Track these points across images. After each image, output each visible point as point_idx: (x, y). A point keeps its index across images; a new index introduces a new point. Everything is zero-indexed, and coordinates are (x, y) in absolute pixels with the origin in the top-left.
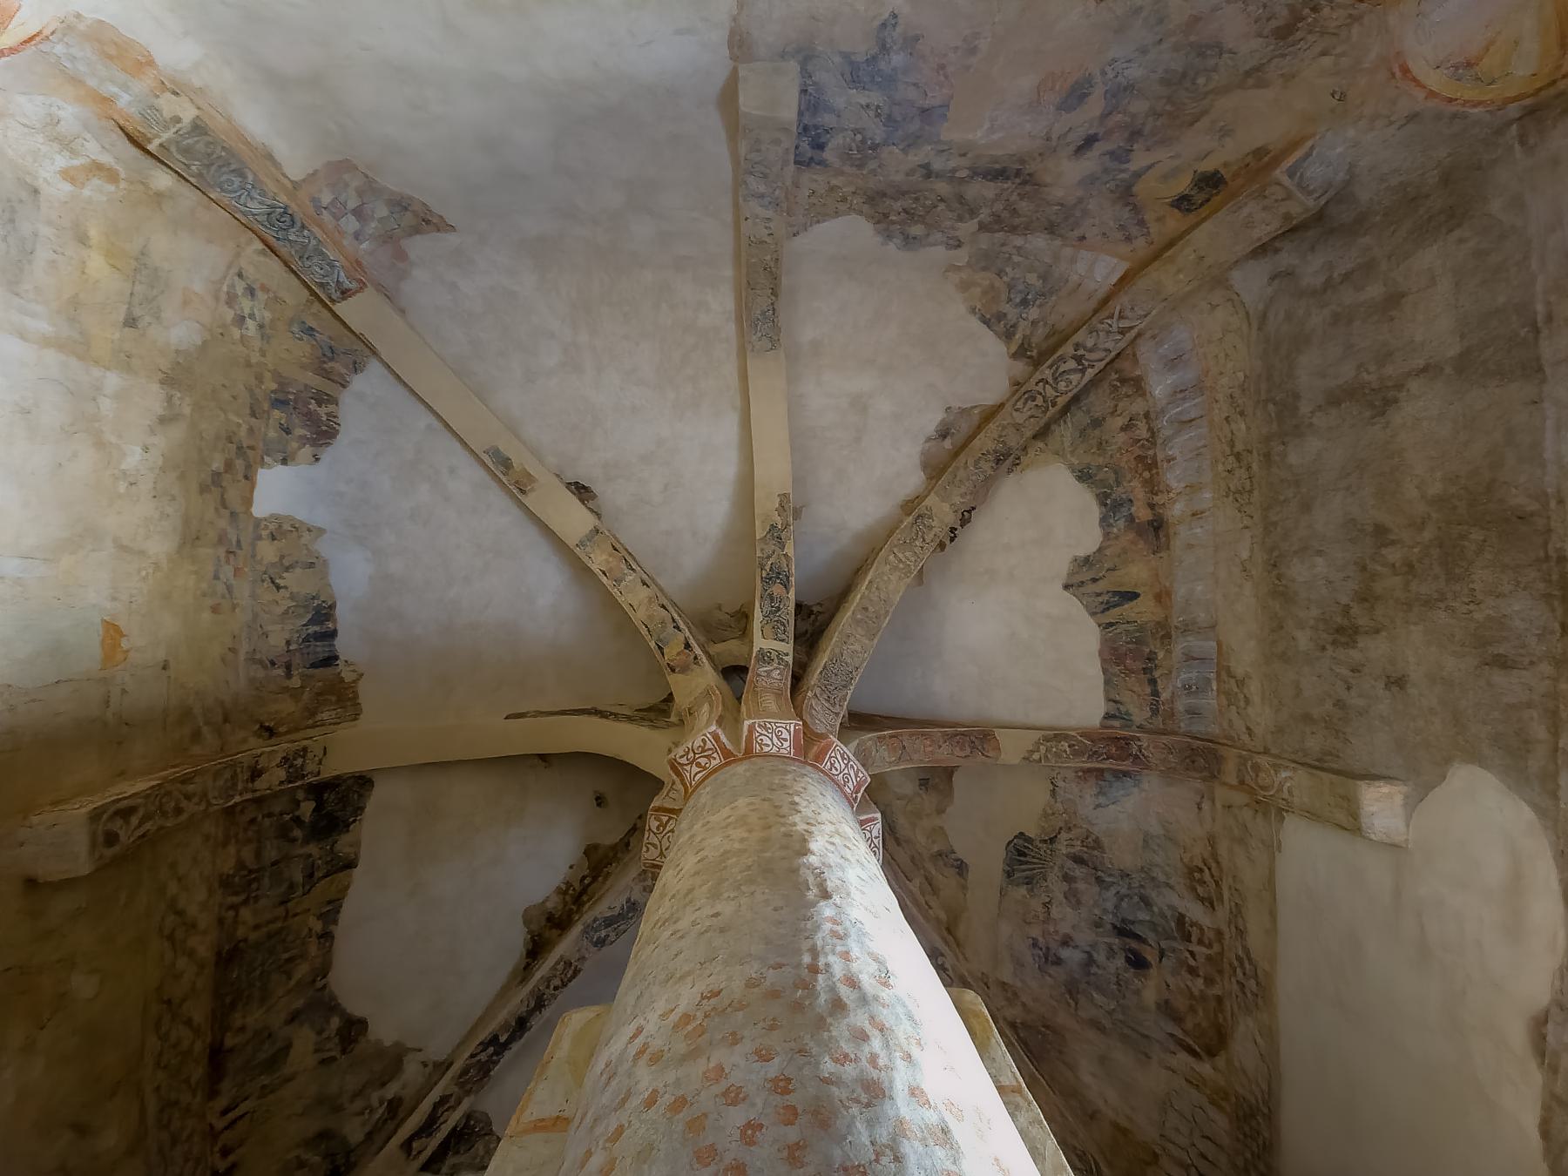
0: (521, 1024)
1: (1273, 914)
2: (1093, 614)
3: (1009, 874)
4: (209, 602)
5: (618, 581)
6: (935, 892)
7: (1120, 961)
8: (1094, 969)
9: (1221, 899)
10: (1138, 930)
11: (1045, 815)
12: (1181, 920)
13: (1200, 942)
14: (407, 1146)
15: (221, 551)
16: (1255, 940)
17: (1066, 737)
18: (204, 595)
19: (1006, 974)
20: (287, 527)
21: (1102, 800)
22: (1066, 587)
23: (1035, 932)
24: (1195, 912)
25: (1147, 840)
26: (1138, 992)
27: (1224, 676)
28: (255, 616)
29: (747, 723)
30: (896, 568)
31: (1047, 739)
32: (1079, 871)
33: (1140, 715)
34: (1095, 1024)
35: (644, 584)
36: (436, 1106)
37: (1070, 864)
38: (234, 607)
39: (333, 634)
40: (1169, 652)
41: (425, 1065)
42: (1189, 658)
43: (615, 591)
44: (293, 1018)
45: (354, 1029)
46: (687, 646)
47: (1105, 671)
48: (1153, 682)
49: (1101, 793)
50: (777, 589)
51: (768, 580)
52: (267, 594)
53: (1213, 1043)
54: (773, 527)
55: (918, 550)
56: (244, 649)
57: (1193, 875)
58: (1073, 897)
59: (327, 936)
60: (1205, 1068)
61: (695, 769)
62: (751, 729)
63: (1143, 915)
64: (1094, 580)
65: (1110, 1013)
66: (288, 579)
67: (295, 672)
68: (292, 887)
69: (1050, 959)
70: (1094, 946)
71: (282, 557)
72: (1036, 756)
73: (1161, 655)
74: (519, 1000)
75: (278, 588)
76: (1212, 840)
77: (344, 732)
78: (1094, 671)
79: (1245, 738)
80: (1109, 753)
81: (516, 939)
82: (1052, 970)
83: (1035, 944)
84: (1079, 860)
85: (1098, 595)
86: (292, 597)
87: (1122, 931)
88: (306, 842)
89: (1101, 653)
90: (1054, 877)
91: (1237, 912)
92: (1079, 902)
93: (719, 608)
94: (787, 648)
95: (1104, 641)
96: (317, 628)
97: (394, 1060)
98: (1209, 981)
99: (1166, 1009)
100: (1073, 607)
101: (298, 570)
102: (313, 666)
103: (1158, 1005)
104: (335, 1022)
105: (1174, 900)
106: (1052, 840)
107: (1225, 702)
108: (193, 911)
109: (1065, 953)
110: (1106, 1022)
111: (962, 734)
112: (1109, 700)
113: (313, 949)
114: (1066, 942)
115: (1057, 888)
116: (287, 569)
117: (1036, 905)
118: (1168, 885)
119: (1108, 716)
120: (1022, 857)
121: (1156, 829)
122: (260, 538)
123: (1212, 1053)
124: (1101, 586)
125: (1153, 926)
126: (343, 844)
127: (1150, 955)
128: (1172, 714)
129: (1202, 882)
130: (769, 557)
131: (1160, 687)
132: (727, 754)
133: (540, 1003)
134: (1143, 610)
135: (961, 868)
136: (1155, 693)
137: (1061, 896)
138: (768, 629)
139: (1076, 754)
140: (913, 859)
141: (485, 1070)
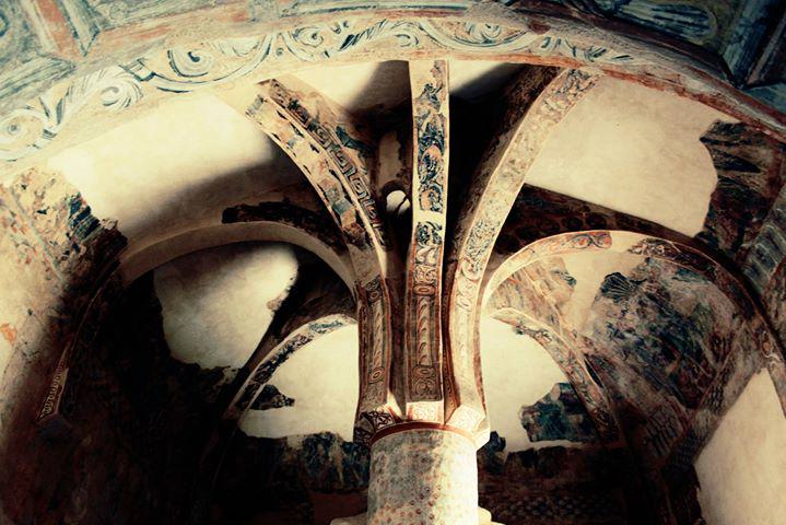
0: (282, 358)
1: (741, 390)
2: (717, 167)
3: (604, 291)
4: (23, 261)
5: (291, 145)
7: (658, 350)
8: (642, 347)
9: (723, 361)
10: (675, 342)
11: (638, 268)
12: (700, 351)
13: (705, 367)
15: (9, 229)
16: (728, 390)
17: (664, 243)
18: (19, 261)
19: (589, 334)
21: (678, 276)
22: (703, 140)
23: (613, 321)
24: (709, 355)
25: (698, 307)
26: (663, 366)
27: (782, 271)
28: (45, 240)
29: (408, 405)
30: (547, 116)
31: (650, 241)
33: (723, 244)
35: (314, 149)
38: (34, 249)
39: (88, 210)
40: (760, 223)
41: (234, 370)
42: (770, 237)
43: (289, 153)
46: (359, 220)
47: (711, 207)
48: (741, 233)
50: (433, 151)
51: (425, 142)
52: (42, 221)
53: (693, 404)
54: (428, 87)
55: (570, 98)
56: (51, 260)
57: (714, 340)
58: (642, 313)
60: (683, 409)
61: (379, 421)
62: (411, 408)
64: (728, 144)
65: (644, 367)
66: (48, 202)
67: (80, 246)
69: (617, 334)
70: (647, 338)
71: (36, 193)
72: (638, 250)
73: (755, 220)
74: (278, 349)
75: (44, 212)
76: (732, 335)
77: (125, 257)
79: (773, 316)
80: (694, 254)
81: (267, 318)
82: (618, 340)
83: (610, 326)
84: (651, 297)
85: (726, 155)
86: (55, 209)
89: (712, 195)
91: (727, 373)
92: (645, 317)
93: (381, 106)
94: (440, 219)
95: (718, 189)
96: (77, 213)
97: (219, 371)
98: (700, 383)
99: (674, 377)
100: (704, 156)
101: (48, 191)
102: (87, 234)
103: (671, 375)
105: (701, 342)
106: (639, 283)
107: (774, 284)
108: (105, 382)
109: (627, 335)
110: (641, 370)
111: (585, 235)
112: (706, 225)
114: (630, 331)
115: (633, 304)
116: (42, 197)
117: (617, 309)
118: (700, 333)
119: (701, 234)
121: (705, 304)
122: (19, 196)
123: (688, 407)
124: (733, 150)
125: (684, 344)
128: (744, 259)
129: (718, 345)
130: (424, 117)
132: (397, 420)
133: (291, 350)
134: (758, 182)
135: (572, 281)
136: (740, 240)
137: (635, 311)
138: (425, 198)
139: (668, 255)
140: (538, 271)
141: (268, 374)
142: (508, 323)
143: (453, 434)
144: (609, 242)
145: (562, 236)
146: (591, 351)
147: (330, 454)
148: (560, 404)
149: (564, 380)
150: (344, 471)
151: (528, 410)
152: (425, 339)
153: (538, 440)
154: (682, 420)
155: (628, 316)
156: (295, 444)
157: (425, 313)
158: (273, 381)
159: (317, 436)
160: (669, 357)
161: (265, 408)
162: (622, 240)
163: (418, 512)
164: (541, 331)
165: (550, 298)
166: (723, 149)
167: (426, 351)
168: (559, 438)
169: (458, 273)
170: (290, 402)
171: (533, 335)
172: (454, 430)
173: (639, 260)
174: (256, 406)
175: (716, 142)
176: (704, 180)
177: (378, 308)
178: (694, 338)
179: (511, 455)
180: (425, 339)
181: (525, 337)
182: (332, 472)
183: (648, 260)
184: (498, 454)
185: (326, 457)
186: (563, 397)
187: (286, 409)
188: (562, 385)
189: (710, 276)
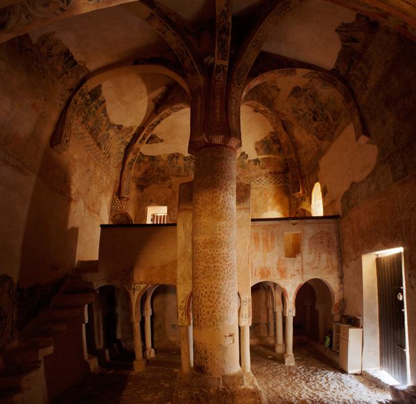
0: (158, 122)
2: (342, 41)
3: (292, 94)
6: (270, 93)
7: (311, 118)
11: (306, 85)
14: (140, 142)
19: (284, 112)
20: (44, 38)
22: (336, 30)
31: (311, 72)
32: (310, 98)
34: (301, 126)
36: (144, 136)
37: (308, 96)
44: (107, 130)
45: (120, 127)
49: (323, 85)
59: (106, 115)
60: (318, 141)
63: (321, 112)
64: (347, 32)
68: (94, 112)
78: (335, 57)
84: (311, 96)
85: (346, 36)
87: (314, 112)
88: (92, 103)
89: (339, 53)
90: (303, 99)
97: (131, 129)
100: (337, 38)
104: (115, 127)
112: (336, 65)
113: (104, 118)
114: (301, 110)
119: (333, 69)
120: (296, 91)
126: (100, 99)
127: (318, 120)
131: (351, 69)
132: (206, 143)
133: (162, 119)
141: (152, 129)
142: (252, 107)
143: (228, 149)
144: (295, 74)
145: (276, 71)
146: (284, 119)
147: (179, 162)
148: (270, 140)
149: (273, 130)
150: (184, 169)
151: (257, 143)
152: (218, 111)
153: (261, 155)
154: (317, 146)
155: (301, 104)
156: (165, 158)
157: (218, 101)
158: (154, 132)
159: (173, 154)
160: (315, 119)
161: (151, 143)
162: (301, 72)
163: (213, 178)
164: (265, 110)
165: (270, 97)
166: (344, 33)
167: (218, 116)
168: (269, 154)
169: (232, 85)
170: (162, 141)
171: (261, 112)
172: (229, 147)
173: (307, 80)
174: (147, 143)
175: (342, 31)
176: (336, 47)
177: (199, 99)
178: (326, 112)
179: (249, 161)
180: (218, 111)
181: (258, 114)
182: (179, 170)
183: (311, 81)
184: (245, 160)
185: (177, 163)
186: (272, 138)
187: (160, 144)
188: (272, 133)
189: (335, 86)
